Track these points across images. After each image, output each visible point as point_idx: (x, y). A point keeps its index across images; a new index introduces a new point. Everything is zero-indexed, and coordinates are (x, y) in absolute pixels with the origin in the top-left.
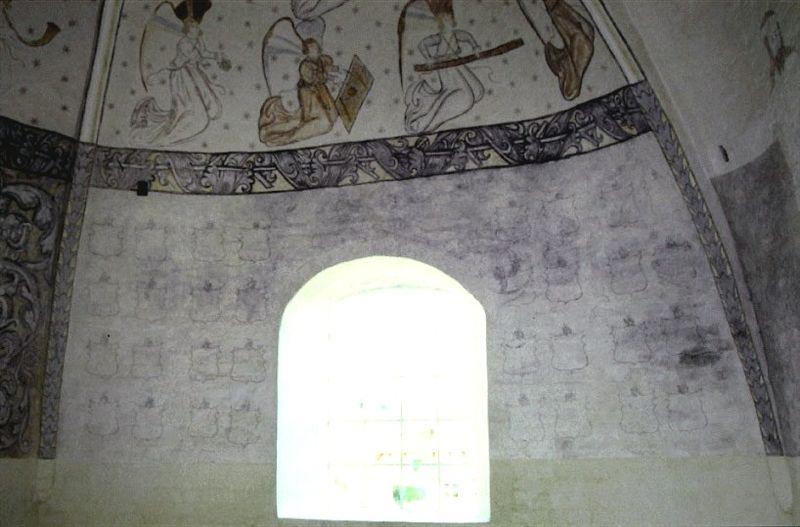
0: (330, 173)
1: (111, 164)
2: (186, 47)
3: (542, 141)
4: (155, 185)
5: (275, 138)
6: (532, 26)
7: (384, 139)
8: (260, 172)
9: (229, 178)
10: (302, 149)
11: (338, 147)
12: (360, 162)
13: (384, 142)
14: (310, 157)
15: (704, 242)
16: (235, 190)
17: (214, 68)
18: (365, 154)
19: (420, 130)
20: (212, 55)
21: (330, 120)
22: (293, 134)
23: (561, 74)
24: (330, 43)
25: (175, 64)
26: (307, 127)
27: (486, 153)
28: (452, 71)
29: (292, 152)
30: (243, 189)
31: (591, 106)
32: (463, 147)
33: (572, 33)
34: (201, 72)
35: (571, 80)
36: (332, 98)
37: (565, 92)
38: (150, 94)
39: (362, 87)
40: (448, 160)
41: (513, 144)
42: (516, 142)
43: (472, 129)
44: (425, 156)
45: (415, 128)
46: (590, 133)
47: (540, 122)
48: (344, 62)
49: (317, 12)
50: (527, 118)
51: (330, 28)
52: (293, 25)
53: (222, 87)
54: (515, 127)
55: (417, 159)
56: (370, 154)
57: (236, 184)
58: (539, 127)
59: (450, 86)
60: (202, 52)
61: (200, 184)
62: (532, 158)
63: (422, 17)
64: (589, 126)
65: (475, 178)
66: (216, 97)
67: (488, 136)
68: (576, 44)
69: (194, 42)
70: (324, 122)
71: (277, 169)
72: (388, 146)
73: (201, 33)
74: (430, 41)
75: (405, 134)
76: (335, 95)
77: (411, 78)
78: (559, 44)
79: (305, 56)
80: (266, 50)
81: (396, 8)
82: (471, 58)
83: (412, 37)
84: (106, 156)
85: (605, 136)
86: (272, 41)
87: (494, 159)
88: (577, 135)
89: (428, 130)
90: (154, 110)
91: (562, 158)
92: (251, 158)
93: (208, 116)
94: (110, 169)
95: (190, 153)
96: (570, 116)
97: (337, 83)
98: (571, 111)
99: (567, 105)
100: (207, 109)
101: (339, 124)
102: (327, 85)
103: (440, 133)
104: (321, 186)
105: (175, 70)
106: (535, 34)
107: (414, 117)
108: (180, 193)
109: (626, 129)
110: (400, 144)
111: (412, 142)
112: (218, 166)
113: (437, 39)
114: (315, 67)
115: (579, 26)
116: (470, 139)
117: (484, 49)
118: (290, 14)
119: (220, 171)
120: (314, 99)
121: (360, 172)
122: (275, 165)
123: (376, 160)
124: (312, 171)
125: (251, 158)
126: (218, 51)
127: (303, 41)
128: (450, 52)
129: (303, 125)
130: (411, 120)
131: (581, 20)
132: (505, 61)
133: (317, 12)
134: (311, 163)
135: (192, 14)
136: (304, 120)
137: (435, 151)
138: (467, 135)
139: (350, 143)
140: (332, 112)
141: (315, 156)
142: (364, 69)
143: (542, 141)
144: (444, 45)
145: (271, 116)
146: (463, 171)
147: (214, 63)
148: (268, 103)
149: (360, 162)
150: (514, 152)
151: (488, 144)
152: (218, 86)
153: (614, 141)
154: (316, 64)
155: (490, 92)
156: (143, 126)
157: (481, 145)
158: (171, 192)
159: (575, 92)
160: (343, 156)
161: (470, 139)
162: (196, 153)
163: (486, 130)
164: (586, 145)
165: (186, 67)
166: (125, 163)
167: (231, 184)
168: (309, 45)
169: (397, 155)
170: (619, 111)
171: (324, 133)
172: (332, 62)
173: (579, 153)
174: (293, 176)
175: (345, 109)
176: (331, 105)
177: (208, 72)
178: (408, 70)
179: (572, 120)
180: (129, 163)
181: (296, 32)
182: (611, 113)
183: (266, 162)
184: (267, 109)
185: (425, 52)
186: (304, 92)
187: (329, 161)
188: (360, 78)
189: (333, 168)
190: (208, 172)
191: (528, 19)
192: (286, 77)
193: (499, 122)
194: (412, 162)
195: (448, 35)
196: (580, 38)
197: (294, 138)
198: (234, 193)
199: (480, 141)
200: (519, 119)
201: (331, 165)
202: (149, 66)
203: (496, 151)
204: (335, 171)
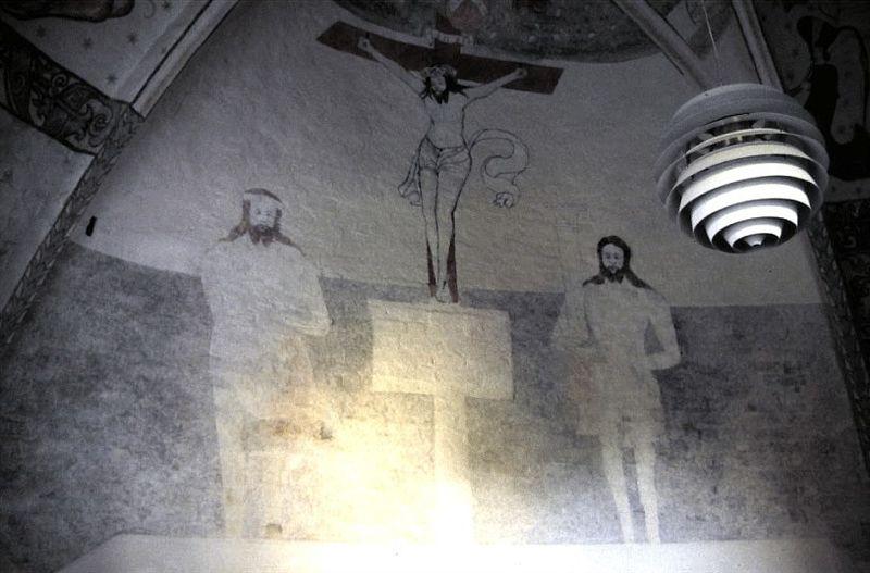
15: (18, 293)
109: (33, 110)
153: (6, 104)
170: (47, 89)
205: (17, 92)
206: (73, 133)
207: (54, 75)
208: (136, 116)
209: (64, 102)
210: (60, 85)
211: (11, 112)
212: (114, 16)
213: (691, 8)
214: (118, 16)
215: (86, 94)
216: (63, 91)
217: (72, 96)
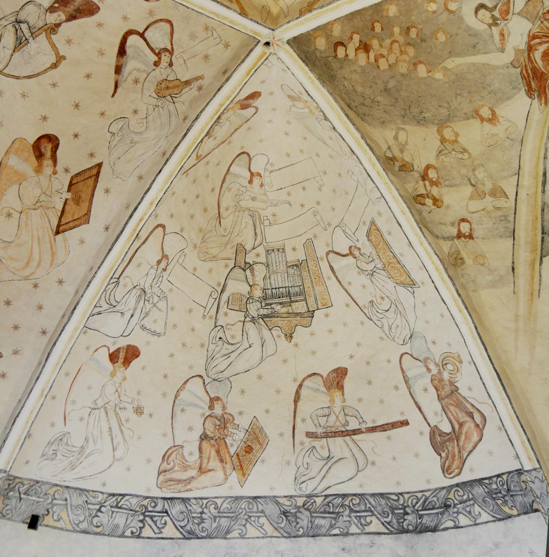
0: (219, 526)
1: (11, 494)
2: (110, 389)
3: (421, 513)
4: (48, 520)
5: (170, 485)
6: (420, 409)
7: (274, 497)
8: (151, 517)
9: (120, 519)
10: (195, 498)
11: (229, 500)
12: (250, 517)
13: (274, 499)
14: (201, 507)
16: (124, 533)
17: (129, 413)
18: (255, 509)
19: (307, 493)
20: (130, 400)
21: (225, 474)
22: (189, 483)
23: (443, 455)
24: (234, 404)
25: (96, 404)
26: (203, 477)
27: (368, 519)
28: (339, 440)
29: (184, 500)
30: (132, 533)
31: (471, 485)
32: (347, 512)
33: (461, 421)
34: (117, 414)
35: (453, 460)
36: (229, 452)
37: (446, 470)
38: (66, 429)
39: (258, 446)
40: (333, 522)
41: (393, 513)
42: (396, 512)
43: (355, 495)
44: (312, 517)
45: (304, 489)
46: (468, 509)
47: (419, 495)
48: (244, 422)
49: (226, 374)
50: (407, 491)
51: (235, 391)
52: (204, 383)
53: (132, 431)
54: (396, 498)
55: (304, 519)
56: (260, 510)
57: (126, 526)
58: (418, 500)
59: (337, 454)
60: (122, 395)
61: (92, 523)
62: (411, 528)
63: (317, 390)
64: (468, 503)
65: (358, 541)
66: (124, 438)
67: (370, 504)
68: (465, 429)
69: (118, 385)
70: (220, 475)
71: (169, 516)
72: (278, 503)
73: (125, 379)
74: (320, 412)
75: (294, 493)
76: (232, 451)
77: (302, 443)
78: (446, 428)
79: (211, 412)
80: (177, 402)
81: (295, 380)
82: (356, 432)
83: (306, 407)
84: (9, 485)
85: (482, 512)
86: (183, 395)
87: (376, 525)
88: (456, 510)
89: (315, 492)
90: (67, 444)
91: (439, 531)
92: (145, 502)
93: (114, 456)
94: (9, 499)
95: (87, 491)
96: (449, 492)
97: (235, 441)
98: (452, 487)
99: (448, 482)
100: (114, 450)
101: (234, 476)
102: (226, 440)
103: (326, 496)
104: (209, 537)
105: (95, 409)
106: (422, 417)
107: (303, 479)
108: (70, 531)
109: (506, 509)
110: (288, 503)
111: (300, 502)
112: (112, 507)
113: (327, 411)
114: (218, 423)
115: (471, 415)
116: (353, 504)
117: (370, 425)
118: (204, 374)
119: (113, 512)
120: (213, 453)
121: (248, 525)
122: (166, 512)
123: (266, 516)
124: (202, 520)
125: (145, 502)
126: (136, 397)
127: (211, 399)
128: (338, 424)
129: (200, 475)
130: (300, 482)
131: (472, 410)
132: (389, 438)
133: (226, 374)
134: (202, 513)
135: (122, 361)
136: (202, 470)
137: (322, 513)
138: (352, 500)
139: (242, 498)
140: (228, 466)
141: (206, 507)
142: (261, 429)
143: (421, 513)
144: (332, 418)
145: (172, 463)
146: (347, 534)
147: (130, 407)
148: (170, 451)
149: (250, 517)
150: (394, 521)
151: (372, 511)
152: (129, 429)
154: (219, 420)
155: (373, 463)
156: (52, 459)
157: (364, 511)
158: (62, 529)
159: (457, 471)
160: (233, 510)
161: (353, 504)
162: (94, 491)
163: (368, 497)
164: (463, 520)
165: (105, 408)
166: (25, 494)
167: (122, 526)
168: (215, 402)
169: (285, 513)
170: (500, 492)
171: (218, 485)
172: (234, 420)
173: (456, 527)
174: (182, 524)
175: (241, 465)
176: (228, 459)
177: (123, 415)
178: (300, 436)
179: (451, 496)
180: (28, 495)
181: (205, 388)
182: (491, 494)
183: (159, 508)
184: (169, 457)
185: (316, 422)
186: (205, 445)
187: (219, 512)
188: (257, 438)
189: (223, 520)
190: (101, 512)
191: (416, 403)
192: (190, 429)
193: (382, 492)
194: (298, 520)
195: (337, 409)
196: (469, 425)
197: (189, 487)
198: (122, 536)
199: (363, 508)
200: (400, 491)
201: (220, 517)
202: (74, 402)
203: (377, 518)
204: (224, 522)
205: (492, 508)
206: (533, 502)
207: (496, 483)
208: (534, 472)
209: (512, 491)
210: (503, 485)
211: (500, 520)
212: (484, 428)
214: (484, 425)
215: (516, 476)
216: (507, 486)
217: (512, 486)
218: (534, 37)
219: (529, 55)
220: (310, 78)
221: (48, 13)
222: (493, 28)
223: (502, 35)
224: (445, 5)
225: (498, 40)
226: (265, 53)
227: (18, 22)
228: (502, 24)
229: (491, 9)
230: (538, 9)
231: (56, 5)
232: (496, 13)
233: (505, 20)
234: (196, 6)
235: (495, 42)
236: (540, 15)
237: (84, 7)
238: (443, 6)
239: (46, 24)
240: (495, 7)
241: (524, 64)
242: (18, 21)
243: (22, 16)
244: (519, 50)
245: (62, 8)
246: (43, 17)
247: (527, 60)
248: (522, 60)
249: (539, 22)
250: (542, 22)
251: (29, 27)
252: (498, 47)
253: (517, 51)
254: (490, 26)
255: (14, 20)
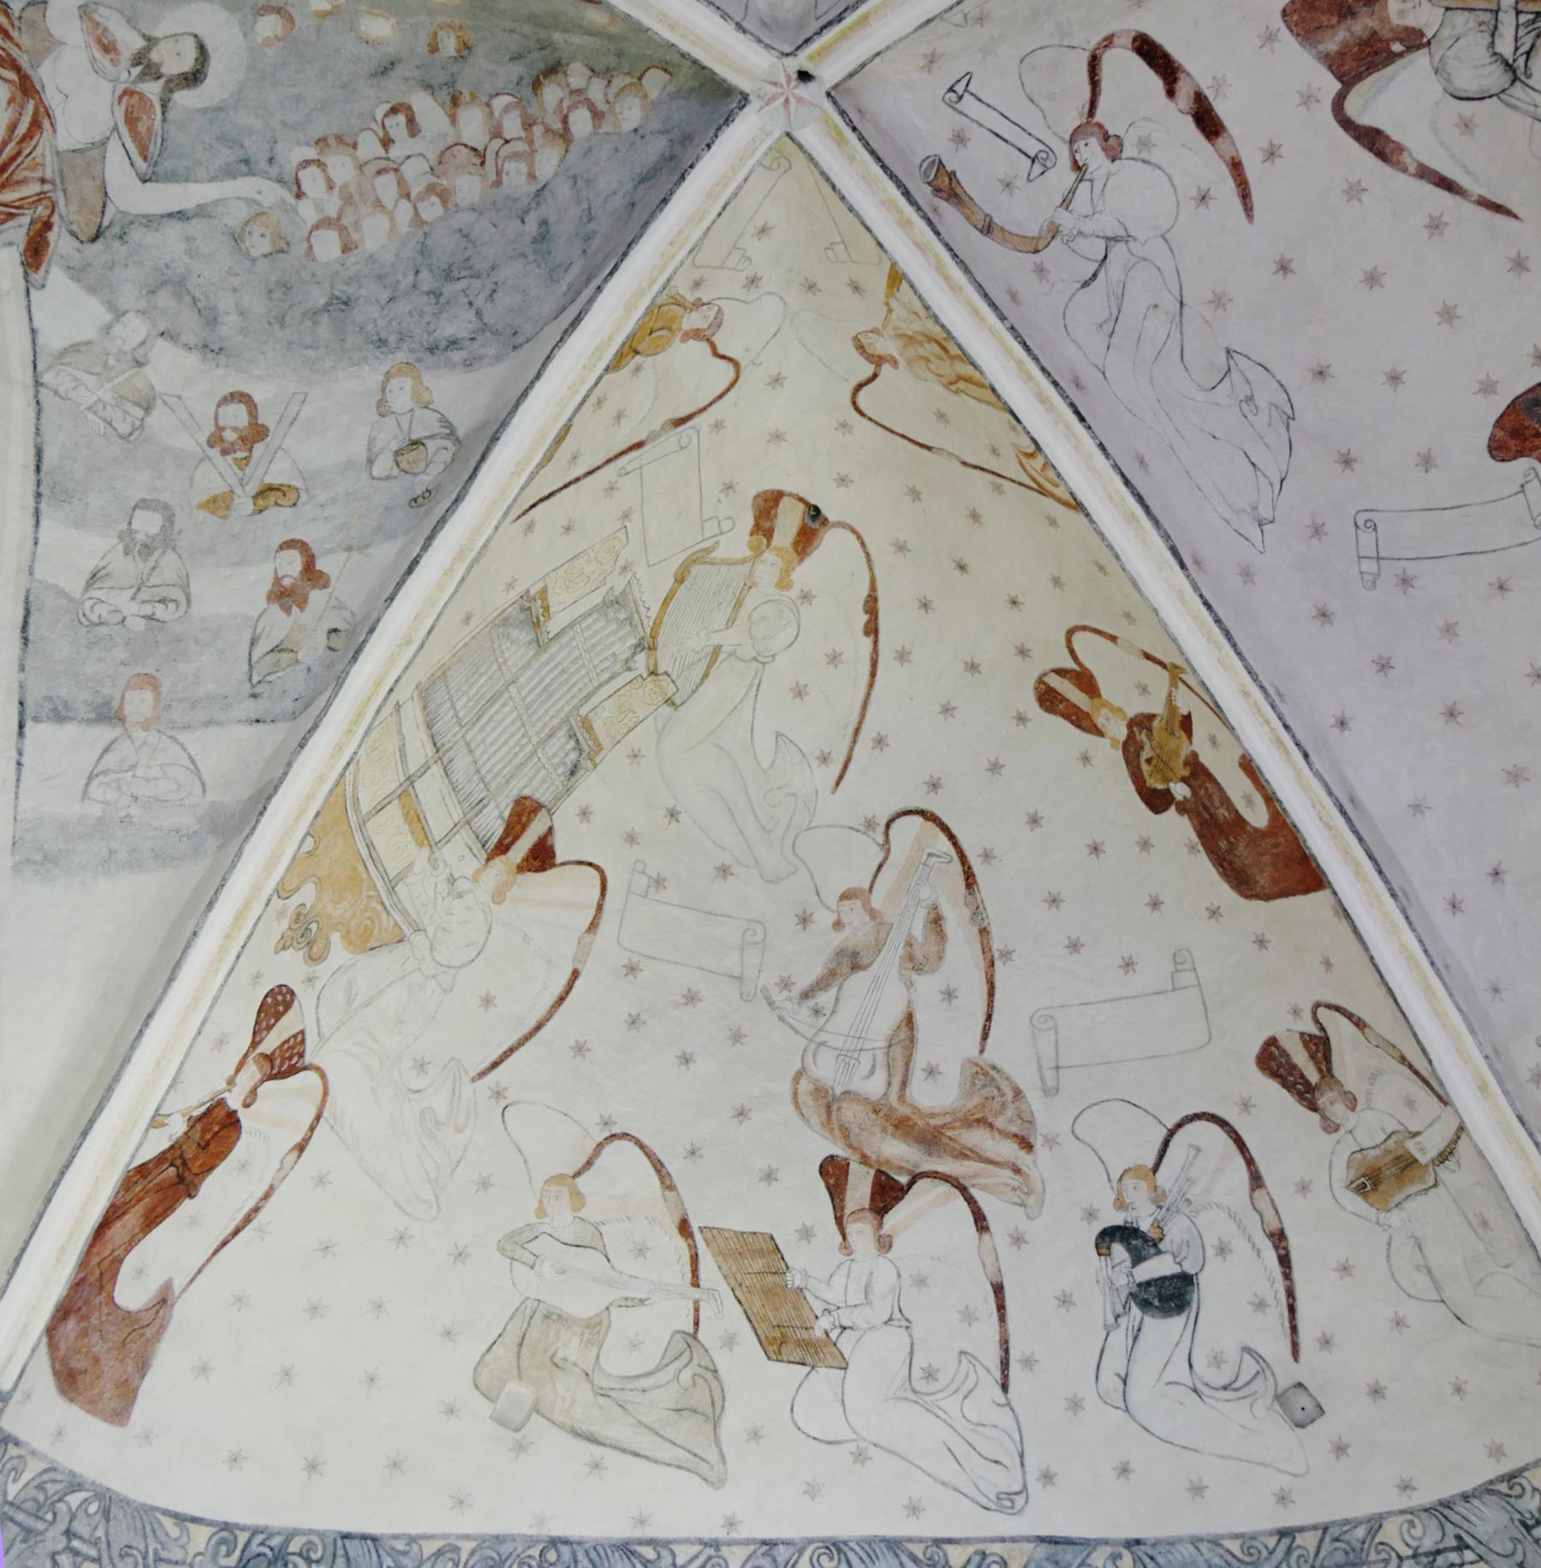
213: (110, 760)
218: (35, 124)
219: (17, 68)
220: (672, 26)
221: (1429, 34)
222: (139, 43)
223: (108, 48)
224: (291, 20)
225: (111, 26)
226: (811, 58)
227: (1514, 72)
228: (124, 76)
229: (171, 91)
230: (73, 208)
231: (1397, 47)
232: (153, 89)
233: (125, 92)
234: (990, 329)
235: (116, 15)
236: (60, 193)
237: (1325, 20)
238: (295, 13)
239: (1447, 9)
240: (165, 105)
241: (15, 34)
242: (1510, 76)
243: (1496, 78)
244: (48, 51)
245: (1385, 34)
246: (1446, 32)
247: (15, 52)
248: (25, 40)
249: (49, 174)
250: (43, 181)
251: (1493, 35)
252: (101, 10)
253: (50, 44)
254: (151, 41)
255: (1518, 84)
